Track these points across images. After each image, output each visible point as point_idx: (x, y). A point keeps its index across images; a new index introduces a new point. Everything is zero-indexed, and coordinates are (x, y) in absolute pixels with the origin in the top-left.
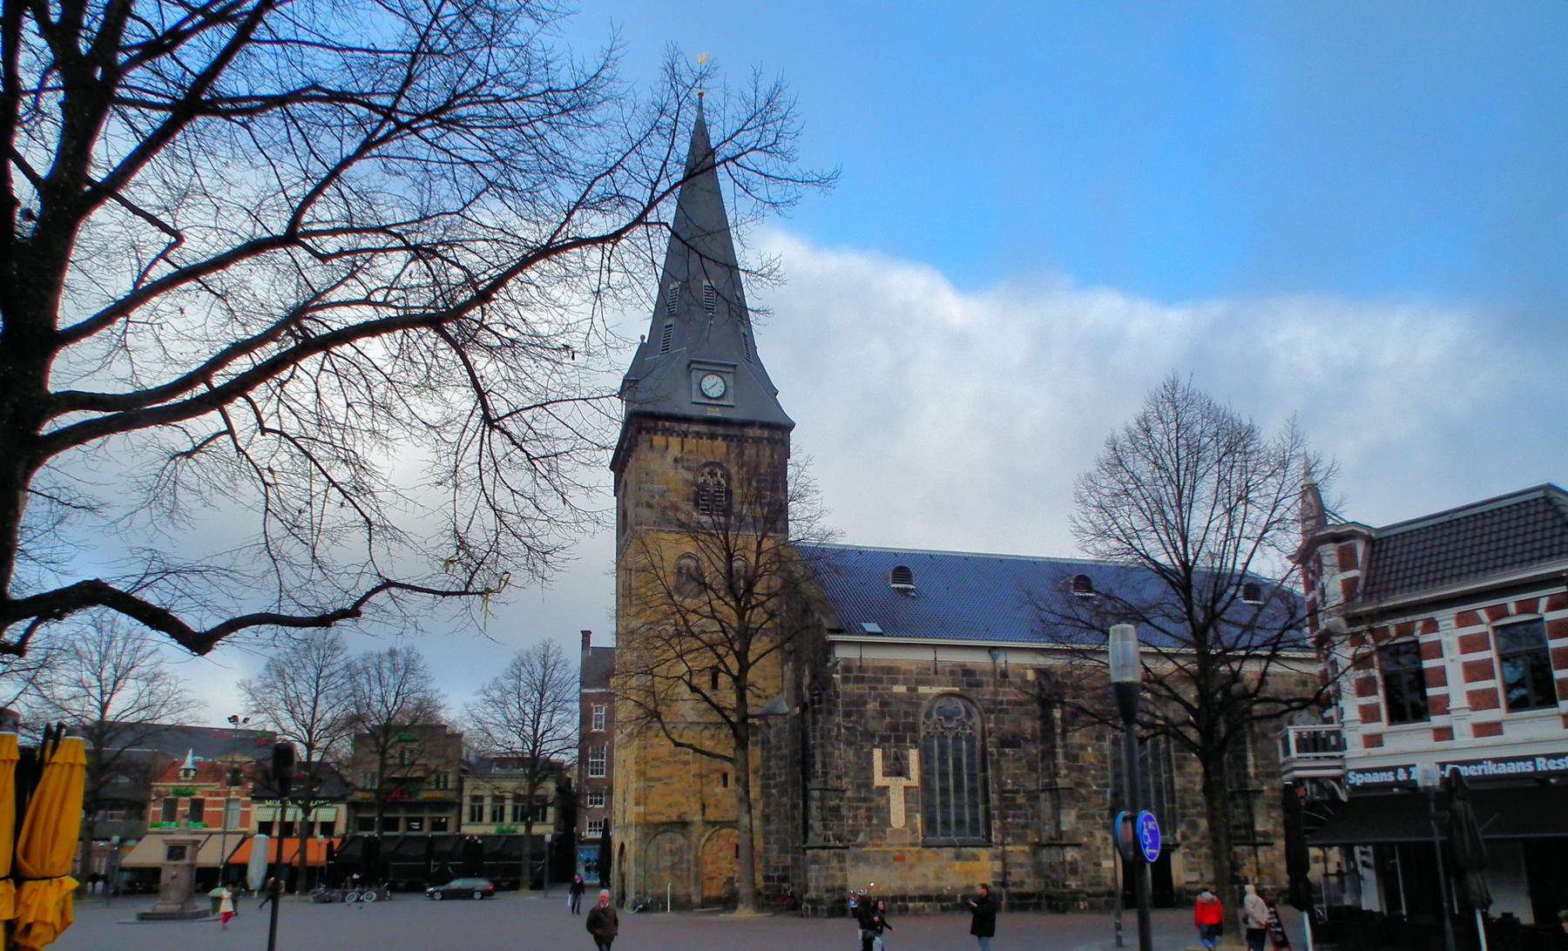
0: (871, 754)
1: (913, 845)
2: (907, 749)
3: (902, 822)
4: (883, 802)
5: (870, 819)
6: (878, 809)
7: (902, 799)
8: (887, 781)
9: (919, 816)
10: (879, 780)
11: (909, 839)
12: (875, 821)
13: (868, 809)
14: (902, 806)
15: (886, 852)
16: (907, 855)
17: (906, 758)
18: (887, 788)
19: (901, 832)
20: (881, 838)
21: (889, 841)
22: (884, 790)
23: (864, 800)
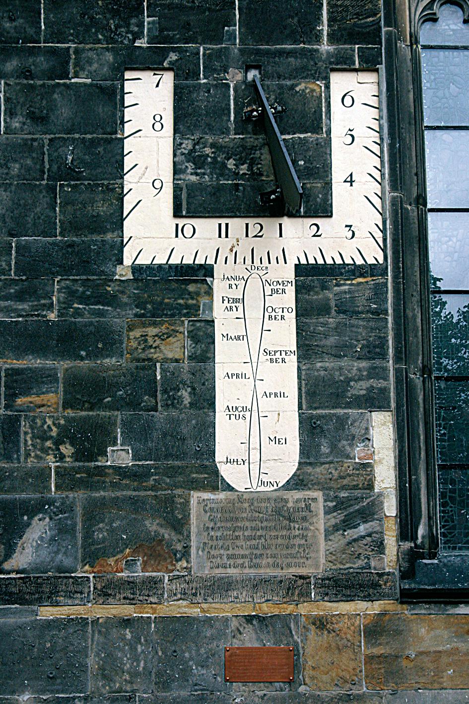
0: (112, 97)
1: (344, 585)
2: (322, 72)
3: (284, 462)
4: (177, 348)
5: (89, 441)
6: (141, 387)
7: (285, 334)
8: (201, 242)
9: (382, 430)
10: (152, 231)
11: (320, 556)
12: (120, 456)
13: (84, 391)
14: (286, 377)
15: (178, 629)
16: (312, 645)
17: (314, 119)
18: (198, 275)
19: (275, 515)
20: (158, 552)
21: (199, 564)
22: (181, 288)
23: (67, 339)
